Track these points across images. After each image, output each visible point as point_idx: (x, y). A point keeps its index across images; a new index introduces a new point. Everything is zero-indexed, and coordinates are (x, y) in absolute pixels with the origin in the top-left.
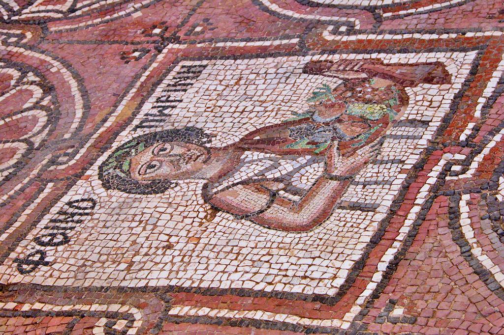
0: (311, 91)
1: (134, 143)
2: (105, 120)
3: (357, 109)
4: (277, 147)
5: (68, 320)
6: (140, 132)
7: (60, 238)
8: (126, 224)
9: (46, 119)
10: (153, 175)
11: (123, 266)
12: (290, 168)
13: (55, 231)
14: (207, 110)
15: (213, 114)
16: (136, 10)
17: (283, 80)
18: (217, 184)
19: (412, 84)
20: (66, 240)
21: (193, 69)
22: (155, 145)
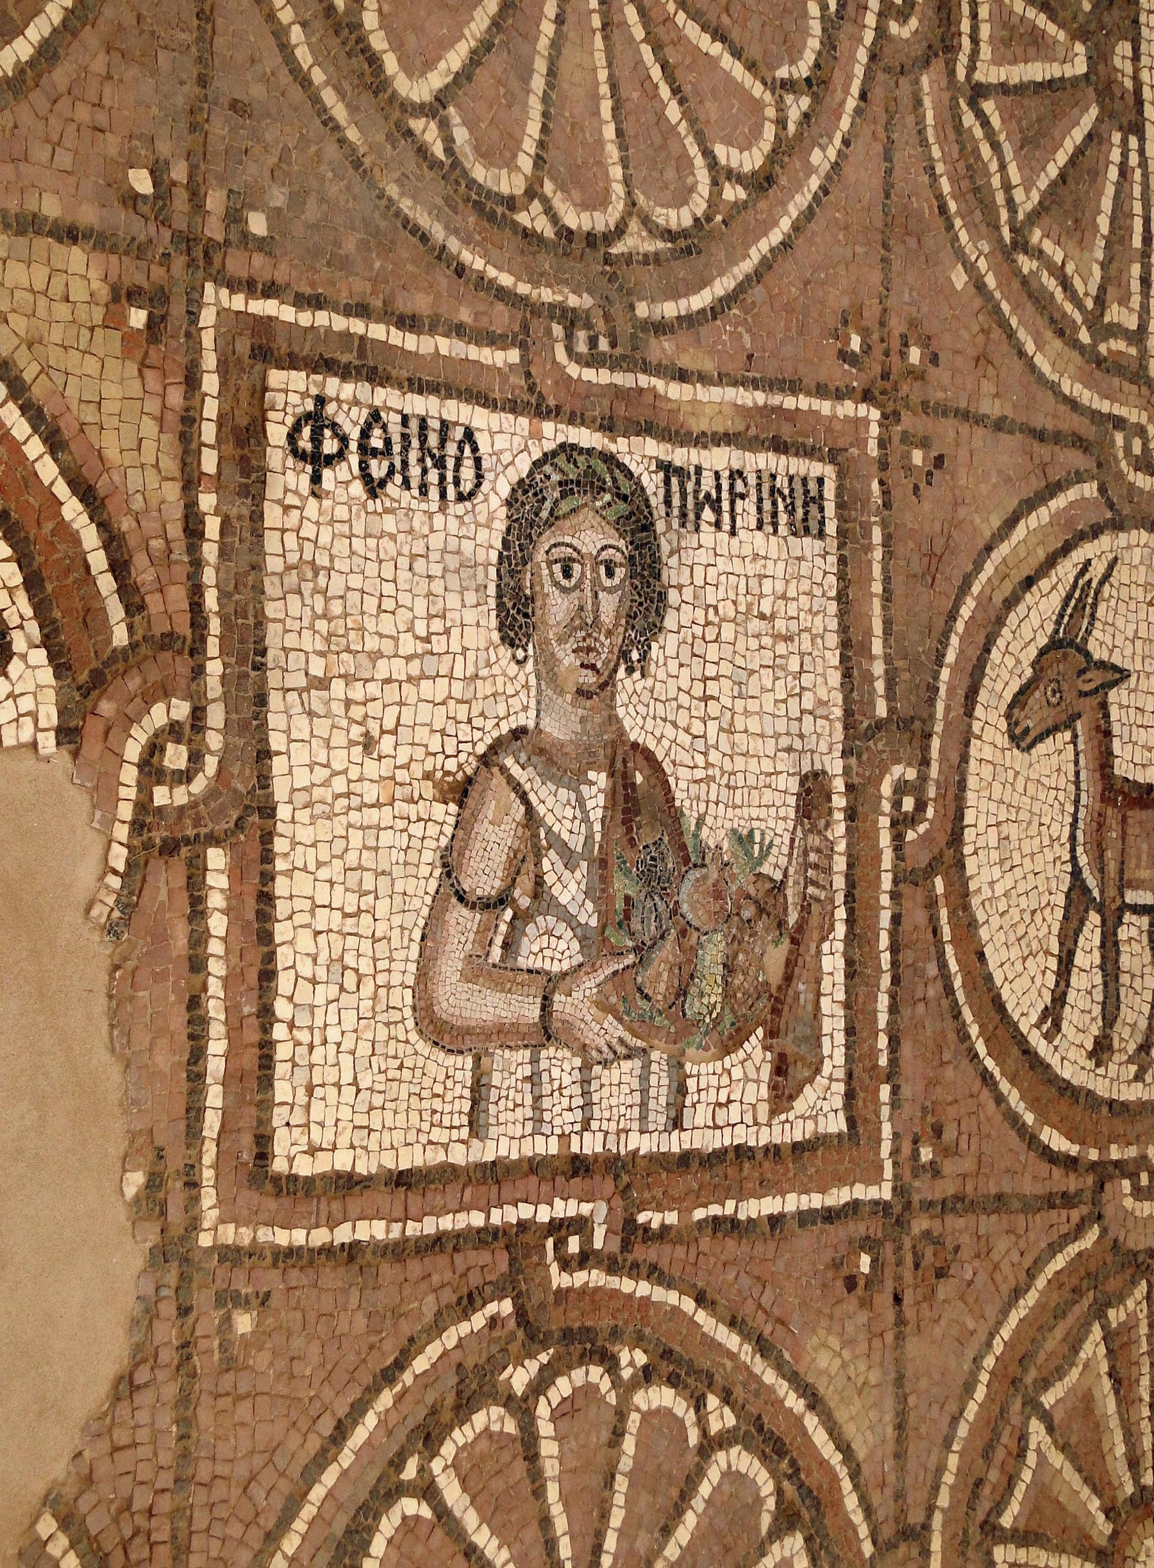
0: (756, 824)
1: (626, 488)
2: (683, 376)
3: (713, 953)
4: (619, 833)
6: (652, 483)
7: (378, 469)
9: (687, 222)
10: (548, 588)
11: (317, 668)
12: (564, 899)
13: (397, 448)
15: (698, 630)
17: (784, 742)
18: (523, 758)
19: (772, 1033)
20: (374, 488)
21: (813, 509)
22: (621, 544)
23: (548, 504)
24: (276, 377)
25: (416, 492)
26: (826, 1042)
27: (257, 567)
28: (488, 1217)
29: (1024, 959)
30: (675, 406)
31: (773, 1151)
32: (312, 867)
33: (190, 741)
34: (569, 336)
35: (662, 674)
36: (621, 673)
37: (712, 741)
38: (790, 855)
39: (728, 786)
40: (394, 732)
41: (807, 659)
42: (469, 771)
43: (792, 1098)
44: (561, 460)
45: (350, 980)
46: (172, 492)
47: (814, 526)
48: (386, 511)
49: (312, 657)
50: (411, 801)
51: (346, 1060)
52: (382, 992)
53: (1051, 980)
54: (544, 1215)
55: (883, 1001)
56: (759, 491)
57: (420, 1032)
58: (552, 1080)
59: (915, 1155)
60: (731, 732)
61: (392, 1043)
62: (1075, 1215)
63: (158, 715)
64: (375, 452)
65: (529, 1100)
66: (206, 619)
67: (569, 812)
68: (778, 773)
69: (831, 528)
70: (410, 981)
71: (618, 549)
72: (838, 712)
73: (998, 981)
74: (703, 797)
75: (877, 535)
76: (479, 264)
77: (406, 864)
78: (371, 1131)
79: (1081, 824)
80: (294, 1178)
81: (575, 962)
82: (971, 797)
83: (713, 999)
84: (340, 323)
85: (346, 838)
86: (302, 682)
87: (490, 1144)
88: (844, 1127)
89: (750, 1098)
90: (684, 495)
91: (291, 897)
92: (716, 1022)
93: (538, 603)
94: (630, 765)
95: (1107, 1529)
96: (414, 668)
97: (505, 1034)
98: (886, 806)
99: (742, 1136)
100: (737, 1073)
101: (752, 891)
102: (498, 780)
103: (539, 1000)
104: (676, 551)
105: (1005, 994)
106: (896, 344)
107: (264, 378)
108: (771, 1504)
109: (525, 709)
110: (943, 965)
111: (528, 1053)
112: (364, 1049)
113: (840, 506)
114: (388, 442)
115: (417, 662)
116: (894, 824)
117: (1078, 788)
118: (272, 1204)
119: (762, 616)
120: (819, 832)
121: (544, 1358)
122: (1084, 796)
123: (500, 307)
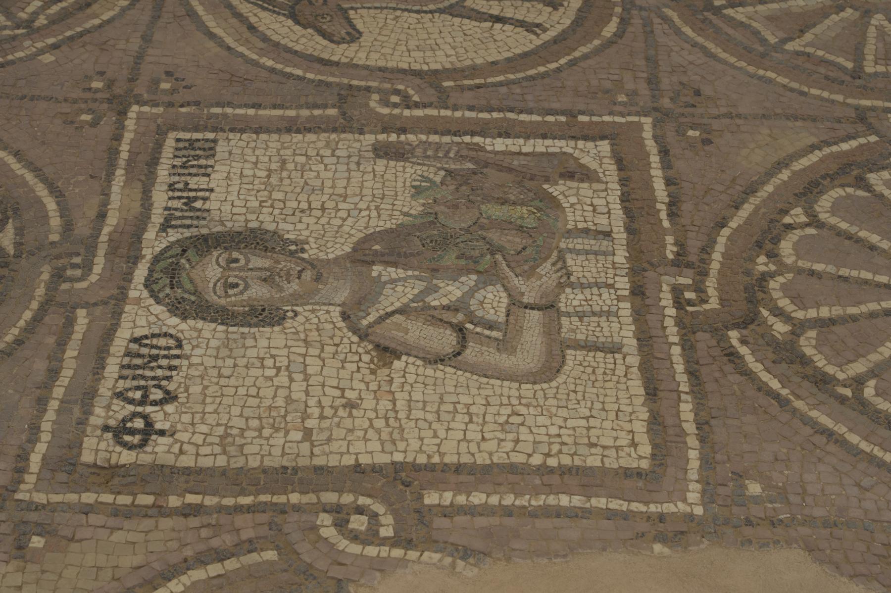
0: (408, 184)
2: (102, 216)
3: (495, 211)
5: (263, 518)
6: (173, 236)
7: (157, 395)
8: (254, 372)
10: (245, 296)
11: (297, 436)
12: (459, 294)
13: (142, 383)
14: (264, 204)
15: (276, 212)
16: (42, 52)
17: (353, 166)
18: (362, 314)
19: (547, 180)
20: (170, 397)
23: (186, 296)
24: (87, 457)
25: (174, 373)
26: (550, 150)
27: (224, 472)
28: (675, 344)
29: (495, 41)
30: (123, 221)
31: (623, 182)
32: (438, 441)
33: (348, 514)
34: (72, 280)
35: (306, 233)
36: (305, 256)
37: (353, 206)
38: (428, 165)
39: (382, 199)
40: (343, 390)
41: (298, 152)
42: (370, 347)
43: (588, 169)
44: (156, 287)
45: (515, 419)
46: (166, 523)
47: (207, 145)
48: (187, 390)
49: (288, 438)
50: (391, 381)
51: (571, 423)
52: (524, 401)
53: (507, 27)
54: (671, 311)
55: (523, 117)
56: (184, 175)
57: (551, 380)
58: (581, 305)
59: (624, 104)
60: (346, 196)
61: (558, 396)
62: (657, 20)
63: (329, 532)
64: (145, 396)
65: (596, 319)
66: (260, 503)
67: (399, 289)
68: (374, 170)
69: (211, 136)
70: (516, 385)
71: (220, 255)
72: (334, 136)
73: (510, 55)
74: (389, 212)
75: (217, 110)
76: (15, 331)
77: (435, 385)
78: (619, 410)
79: (409, 7)
80: (653, 456)
81: (502, 289)
82: (390, 65)
83: (525, 211)
84: (50, 415)
85: (417, 420)
86: (307, 445)
87: (625, 341)
88: (607, 142)
89: (590, 193)
90: (183, 218)
91: (459, 454)
92: (539, 210)
93: (255, 303)
94: (367, 252)
95: (849, 11)
96: (298, 377)
97: (551, 331)
98: (396, 111)
99: (614, 198)
100: (573, 200)
101: (453, 187)
102: (378, 329)
103: (527, 311)
104: (222, 223)
105: (518, 51)
106: (88, 95)
107: (88, 466)
108: (850, 190)
109: (328, 312)
110: (501, 84)
111: (563, 319)
112: (563, 413)
113: (196, 129)
114: (138, 388)
115: (294, 375)
116: (408, 107)
117: (386, 8)
118: (671, 471)
119: (269, 176)
120: (414, 149)
121: (765, 313)
122: (390, 5)
123: (47, 319)
